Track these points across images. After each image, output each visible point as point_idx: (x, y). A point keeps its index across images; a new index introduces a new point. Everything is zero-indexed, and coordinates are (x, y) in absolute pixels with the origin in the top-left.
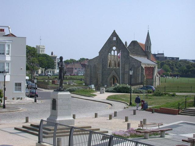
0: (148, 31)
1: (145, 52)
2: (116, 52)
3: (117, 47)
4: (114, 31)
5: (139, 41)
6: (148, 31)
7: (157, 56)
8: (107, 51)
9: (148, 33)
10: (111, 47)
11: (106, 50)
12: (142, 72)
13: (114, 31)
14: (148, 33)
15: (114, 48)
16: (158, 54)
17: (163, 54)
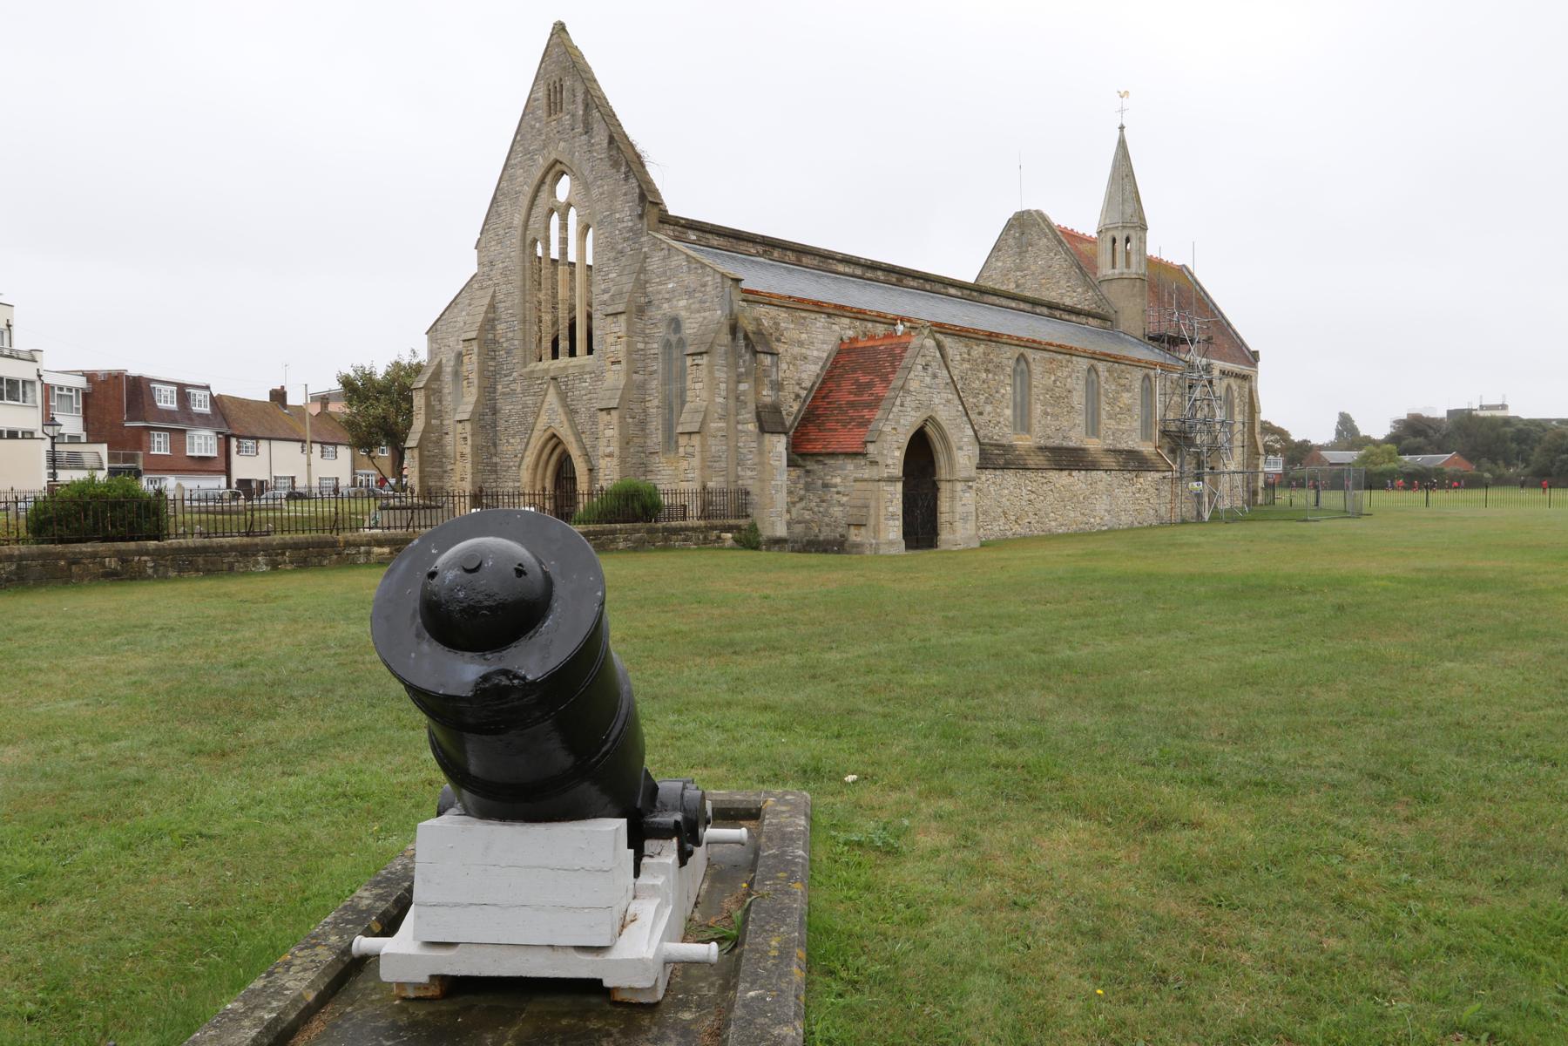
0: (1122, 128)
4: (560, 29)
5: (1059, 218)
6: (1122, 128)
9: (1122, 144)
10: (542, 182)
13: (560, 29)
14: (1122, 144)
16: (1482, 407)
17: (1504, 407)
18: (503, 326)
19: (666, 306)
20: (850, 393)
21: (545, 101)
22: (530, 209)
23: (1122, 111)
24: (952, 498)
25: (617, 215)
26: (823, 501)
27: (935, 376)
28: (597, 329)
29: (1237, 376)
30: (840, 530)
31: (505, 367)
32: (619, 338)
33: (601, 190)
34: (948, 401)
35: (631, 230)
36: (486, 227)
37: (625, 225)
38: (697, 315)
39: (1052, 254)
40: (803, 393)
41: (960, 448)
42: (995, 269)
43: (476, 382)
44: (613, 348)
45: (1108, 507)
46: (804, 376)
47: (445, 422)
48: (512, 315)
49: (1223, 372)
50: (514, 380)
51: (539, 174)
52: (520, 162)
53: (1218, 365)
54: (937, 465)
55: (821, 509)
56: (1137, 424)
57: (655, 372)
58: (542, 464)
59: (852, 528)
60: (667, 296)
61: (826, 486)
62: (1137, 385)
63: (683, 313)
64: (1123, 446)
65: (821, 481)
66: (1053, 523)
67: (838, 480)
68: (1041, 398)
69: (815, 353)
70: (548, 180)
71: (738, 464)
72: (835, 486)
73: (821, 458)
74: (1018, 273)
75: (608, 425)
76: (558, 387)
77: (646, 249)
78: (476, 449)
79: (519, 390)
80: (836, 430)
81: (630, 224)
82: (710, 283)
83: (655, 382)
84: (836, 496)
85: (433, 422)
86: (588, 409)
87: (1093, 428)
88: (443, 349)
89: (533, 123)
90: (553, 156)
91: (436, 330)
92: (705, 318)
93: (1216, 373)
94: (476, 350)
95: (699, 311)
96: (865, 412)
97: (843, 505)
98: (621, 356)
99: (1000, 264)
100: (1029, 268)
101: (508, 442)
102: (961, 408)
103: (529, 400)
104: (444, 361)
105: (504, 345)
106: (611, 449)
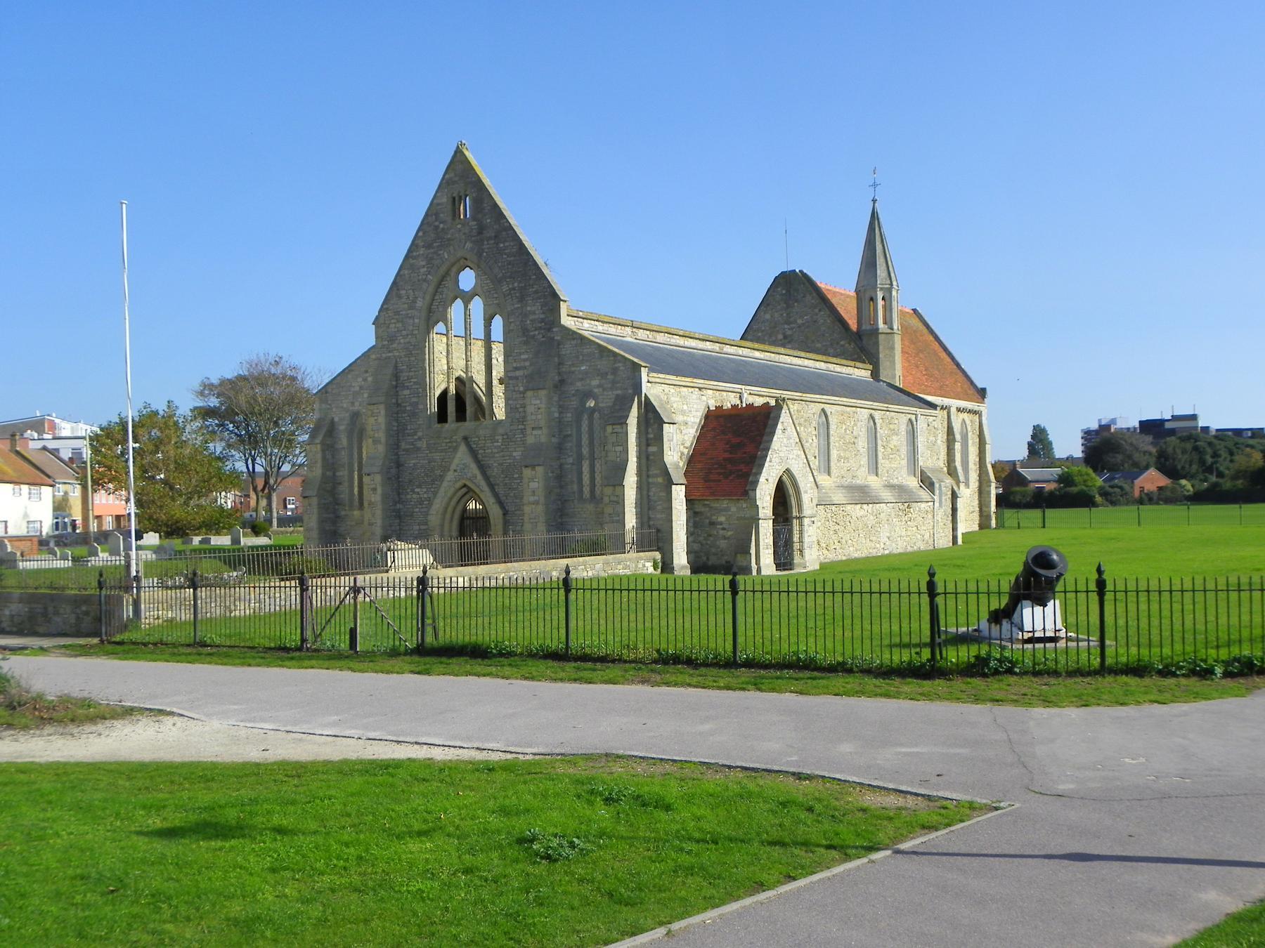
0: (874, 201)
1: (858, 336)
2: (477, 305)
3: (476, 267)
6: (874, 201)
7: (1168, 425)
8: (419, 304)
9: (874, 216)
10: (447, 273)
11: (414, 302)
12: (652, 449)
14: (874, 216)
15: (467, 279)
16: (1175, 418)
17: (1194, 417)
18: (406, 392)
19: (579, 384)
20: (725, 451)
21: (450, 207)
23: (875, 185)
24: (801, 532)
25: (529, 308)
26: (710, 536)
27: (789, 438)
29: (970, 412)
30: (726, 558)
31: (409, 428)
34: (798, 456)
35: (542, 321)
36: (385, 307)
37: (537, 317)
38: (610, 393)
39: (817, 311)
40: (686, 451)
41: (806, 492)
42: (764, 322)
43: (383, 440)
44: (533, 417)
45: (888, 535)
46: (686, 438)
47: (338, 474)
49: (959, 410)
50: (420, 439)
53: (955, 403)
54: (789, 504)
55: (709, 542)
56: (904, 462)
57: (568, 436)
58: (450, 509)
59: (739, 555)
60: (580, 376)
61: (712, 524)
62: (903, 428)
63: (596, 390)
64: (895, 482)
65: (708, 521)
66: (851, 549)
67: (722, 519)
68: (837, 444)
69: (692, 420)
70: (454, 269)
71: (649, 509)
72: (721, 523)
73: (708, 503)
74: (786, 326)
75: (532, 480)
77: (559, 338)
78: (385, 497)
80: (720, 481)
81: (542, 316)
82: (622, 368)
83: (570, 444)
84: (721, 532)
85: (328, 473)
86: (502, 464)
87: (875, 468)
88: (334, 410)
89: (437, 223)
90: (459, 254)
91: (326, 392)
92: (617, 395)
93: (953, 410)
94: (383, 412)
95: (612, 389)
96: (742, 466)
97: (728, 538)
98: (542, 423)
99: (768, 316)
100: (795, 322)
102: (805, 461)
103: (437, 456)
104: (336, 419)
106: (536, 498)
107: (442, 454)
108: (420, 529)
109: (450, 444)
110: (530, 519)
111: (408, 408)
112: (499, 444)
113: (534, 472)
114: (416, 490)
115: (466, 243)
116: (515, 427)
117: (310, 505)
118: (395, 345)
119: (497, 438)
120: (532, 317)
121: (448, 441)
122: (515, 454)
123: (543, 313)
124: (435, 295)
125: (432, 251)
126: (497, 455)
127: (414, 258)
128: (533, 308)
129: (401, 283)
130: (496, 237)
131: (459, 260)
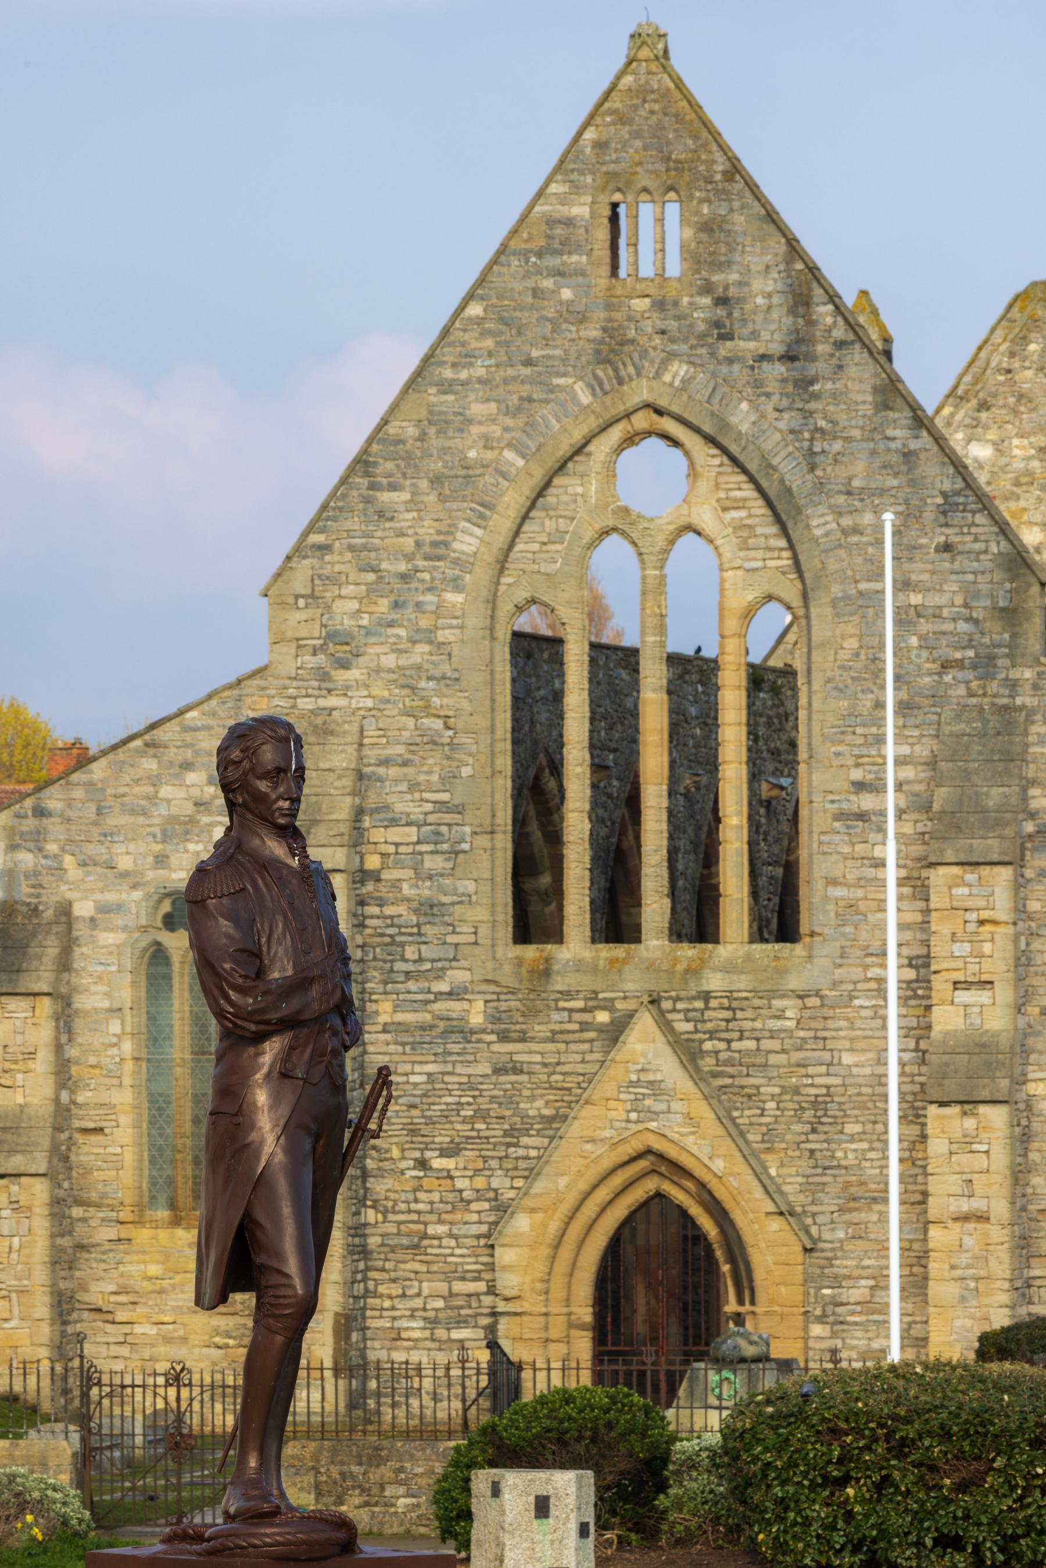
21: (602, 234)
22: (525, 517)
28: (832, 882)
31: (410, 952)
32: (982, 922)
33: (846, 521)
37: (948, 627)
44: (961, 949)
48: (442, 807)
51: (577, 435)
52: (480, 381)
70: (601, 448)
76: (666, 1026)
79: (477, 1018)
86: (796, 1091)
90: (641, 391)
91: (40, 812)
101: (422, 1164)
104: (83, 909)
105: (406, 889)
106: (977, 1204)
107: (550, 1047)
108: (451, 1294)
109: (586, 1017)
110: (953, 1267)
111: (406, 889)
112: (790, 1024)
113: (970, 1123)
114: (437, 1163)
115: (664, 364)
116: (857, 973)
117: (15, 1205)
118: (355, 674)
119: (777, 1003)
120: (924, 626)
121: (580, 1004)
122: (847, 1059)
123: (969, 619)
124: (525, 517)
125: (527, 371)
126: (773, 1059)
127: (446, 387)
128: (935, 600)
129: (389, 466)
130: (789, 358)
131: (628, 416)
